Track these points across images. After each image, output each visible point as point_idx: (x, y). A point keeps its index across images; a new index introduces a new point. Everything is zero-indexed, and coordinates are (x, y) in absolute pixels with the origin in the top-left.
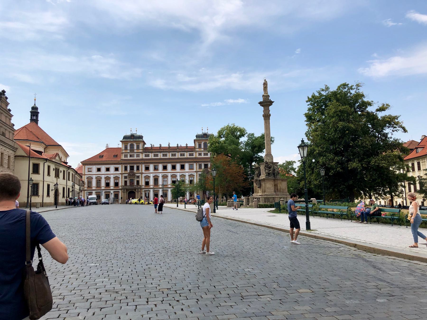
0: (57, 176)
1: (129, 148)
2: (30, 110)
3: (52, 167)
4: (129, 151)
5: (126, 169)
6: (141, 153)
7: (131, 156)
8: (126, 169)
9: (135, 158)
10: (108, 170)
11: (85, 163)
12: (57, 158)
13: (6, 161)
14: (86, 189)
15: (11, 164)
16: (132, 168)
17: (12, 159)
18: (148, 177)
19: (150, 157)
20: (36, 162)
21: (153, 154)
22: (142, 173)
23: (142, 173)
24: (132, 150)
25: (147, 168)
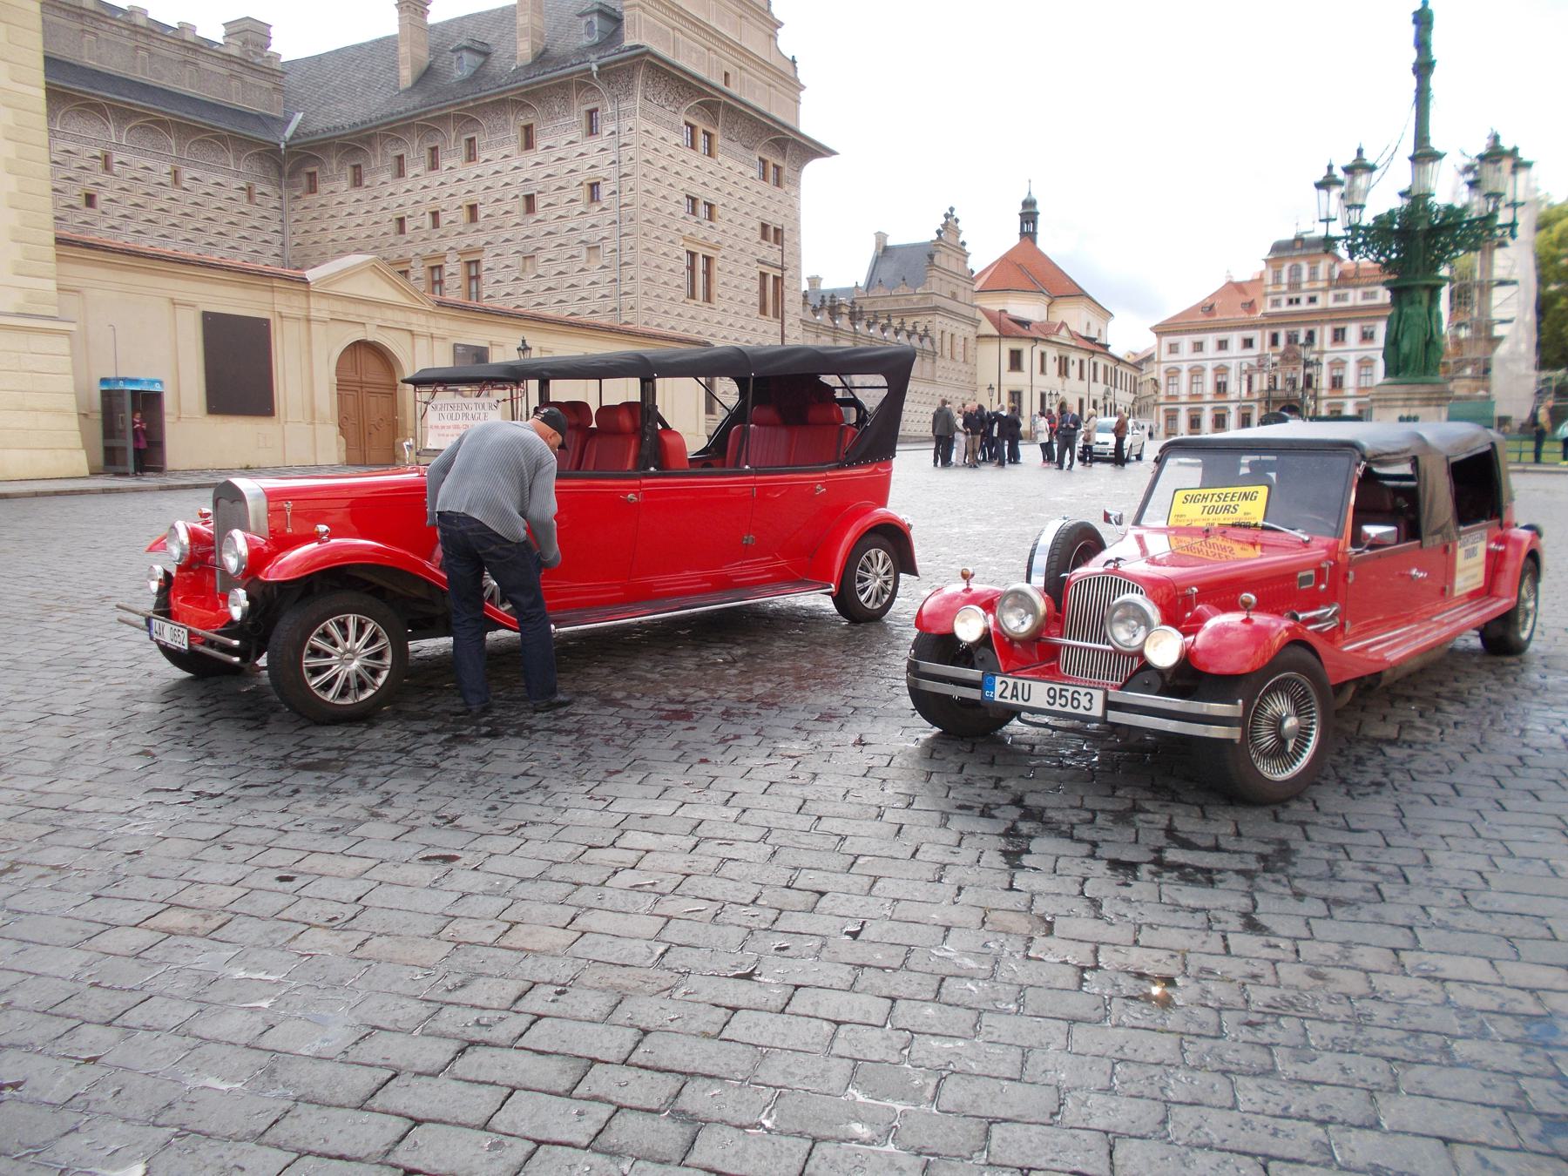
0: (1063, 371)
1: (1285, 278)
2: (1019, 208)
3: (1052, 353)
4: (1284, 288)
5: (1274, 340)
6: (1323, 290)
7: (1290, 302)
8: (1274, 340)
9: (1304, 306)
10: (1222, 345)
11: (1161, 330)
12: (1063, 332)
13: (959, 349)
14: (1162, 400)
15: (970, 352)
16: (1292, 339)
17: (971, 344)
18: (1339, 364)
19: (1349, 303)
20: (1016, 345)
21: (1359, 292)
22: (1322, 352)
23: (1322, 352)
24: (1294, 285)
25: (1339, 336)
